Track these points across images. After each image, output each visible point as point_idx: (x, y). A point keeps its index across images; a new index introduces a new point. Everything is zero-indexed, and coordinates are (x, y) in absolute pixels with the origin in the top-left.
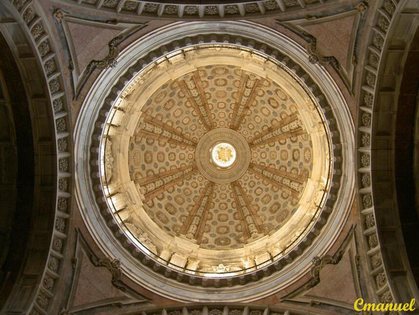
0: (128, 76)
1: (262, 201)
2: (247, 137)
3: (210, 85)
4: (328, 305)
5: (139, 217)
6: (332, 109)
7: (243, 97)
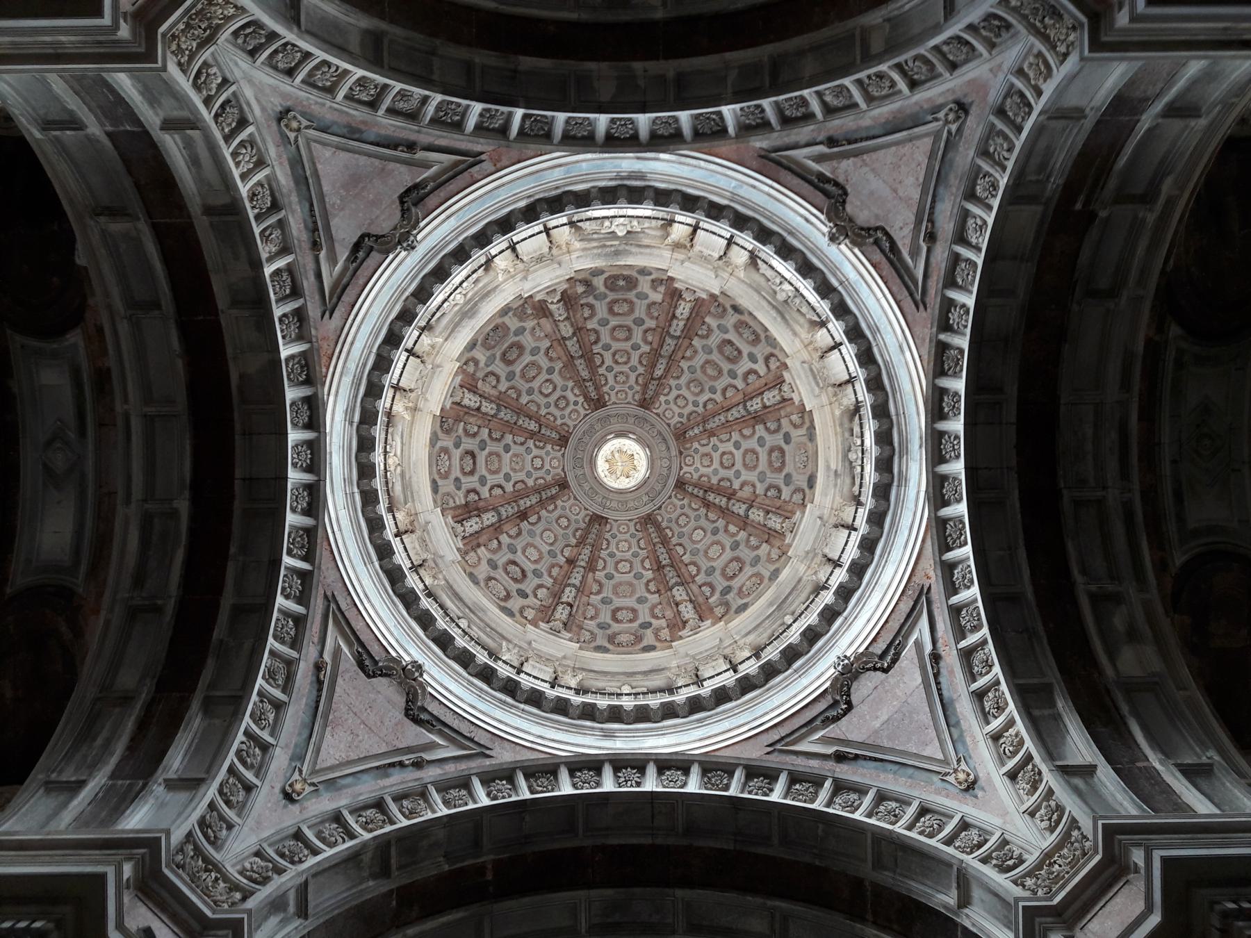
0: (812, 636)
1: (540, 368)
2: (572, 501)
3: (647, 611)
4: (378, 145)
5: (795, 334)
6: (377, 564)
7: (578, 583)
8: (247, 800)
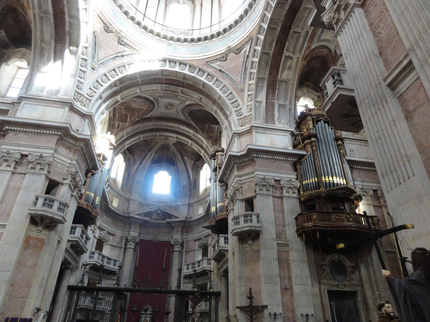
8: (84, 75)
